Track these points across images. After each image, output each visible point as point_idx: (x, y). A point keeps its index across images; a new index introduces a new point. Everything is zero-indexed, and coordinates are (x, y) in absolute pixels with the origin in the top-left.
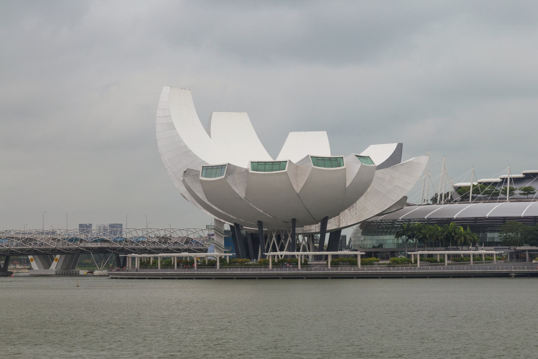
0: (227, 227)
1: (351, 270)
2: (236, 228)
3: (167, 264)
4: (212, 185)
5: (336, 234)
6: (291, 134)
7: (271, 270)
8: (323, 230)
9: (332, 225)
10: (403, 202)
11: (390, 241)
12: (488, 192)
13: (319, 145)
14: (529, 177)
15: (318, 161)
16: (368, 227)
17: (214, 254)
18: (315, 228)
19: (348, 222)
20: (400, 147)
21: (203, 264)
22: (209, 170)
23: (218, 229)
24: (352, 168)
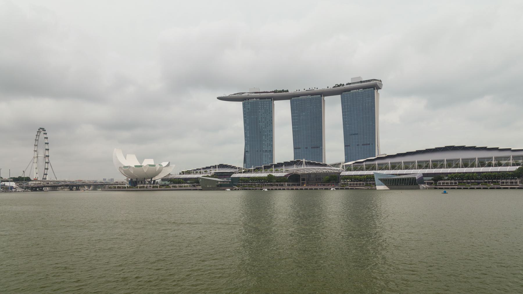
0: (129, 179)
1: (157, 189)
2: (131, 180)
3: (115, 188)
4: (125, 170)
5: (154, 181)
6: (145, 160)
7: (139, 189)
8: (151, 180)
9: (153, 179)
10: (169, 174)
11: (167, 183)
12: (189, 172)
13: (151, 162)
14: (197, 169)
15: (150, 165)
16: (163, 180)
17: (126, 185)
18: (150, 180)
19: (158, 179)
20: (169, 163)
21: (123, 188)
22: (125, 167)
23: (127, 180)
24: (158, 167)
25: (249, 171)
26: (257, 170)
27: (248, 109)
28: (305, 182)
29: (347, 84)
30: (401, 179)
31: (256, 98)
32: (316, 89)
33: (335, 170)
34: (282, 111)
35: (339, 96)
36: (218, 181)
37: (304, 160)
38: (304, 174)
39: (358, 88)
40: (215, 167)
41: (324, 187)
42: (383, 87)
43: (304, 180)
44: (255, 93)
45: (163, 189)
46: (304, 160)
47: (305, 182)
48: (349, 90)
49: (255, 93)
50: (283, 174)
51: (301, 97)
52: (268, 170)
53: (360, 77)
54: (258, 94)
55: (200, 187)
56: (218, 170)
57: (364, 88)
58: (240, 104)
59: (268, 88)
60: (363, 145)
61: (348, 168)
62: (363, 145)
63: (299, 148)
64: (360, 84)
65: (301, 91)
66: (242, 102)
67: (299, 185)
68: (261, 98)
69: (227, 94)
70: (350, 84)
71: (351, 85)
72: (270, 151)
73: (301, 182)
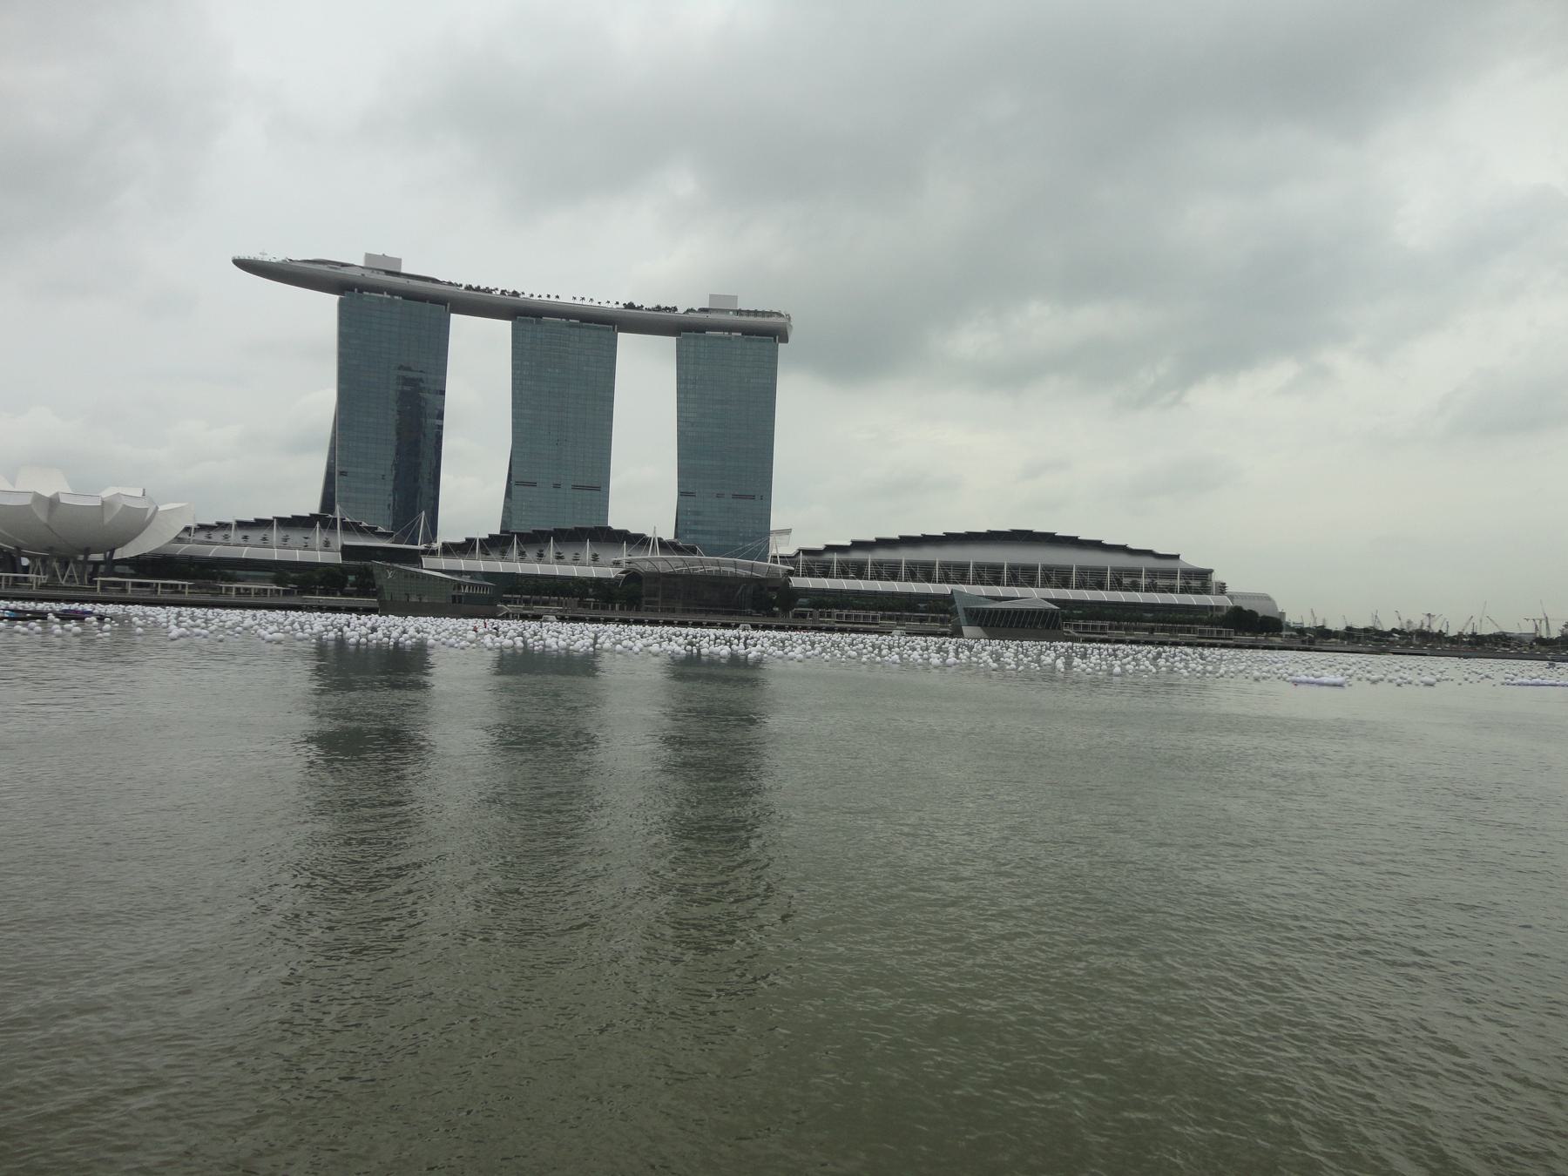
28: (659, 599)
29: (692, 310)
30: (1003, 611)
31: (392, 291)
32: (595, 303)
33: (744, 567)
35: (670, 342)
38: (657, 577)
39: (730, 328)
42: (790, 339)
44: (388, 273)
45: (195, 598)
47: (659, 599)
49: (388, 273)
50: (612, 573)
52: (531, 554)
53: (736, 298)
55: (372, 602)
57: (748, 331)
58: (332, 300)
63: (534, 484)
66: (336, 298)
67: (638, 610)
69: (274, 254)
71: (711, 316)
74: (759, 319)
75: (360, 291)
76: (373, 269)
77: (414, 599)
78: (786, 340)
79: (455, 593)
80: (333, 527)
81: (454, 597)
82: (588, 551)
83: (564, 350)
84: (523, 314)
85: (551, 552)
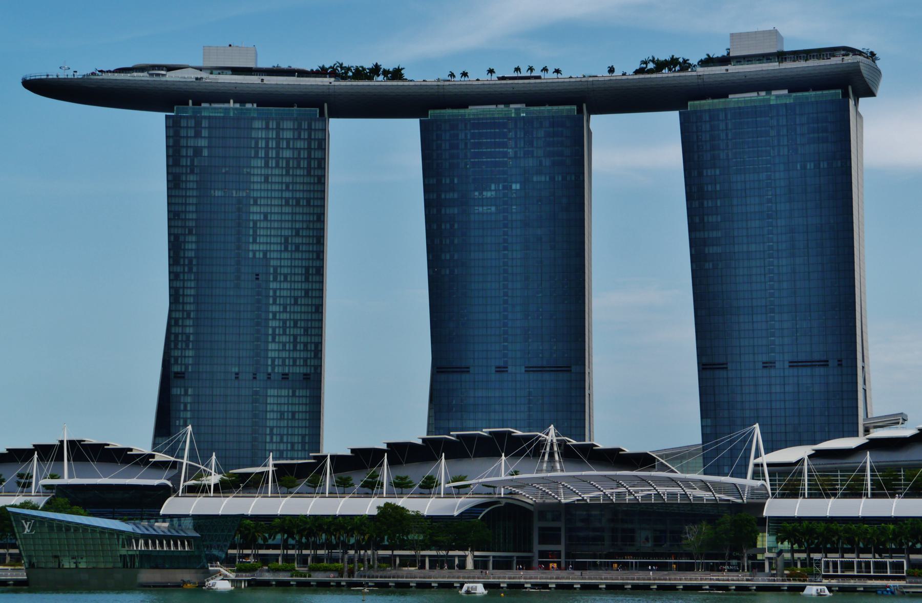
25: (250, 484)
26: (288, 478)
27: (197, 151)
29: (708, 61)
31: (242, 97)
32: (550, 76)
34: (375, 177)
36: (129, 538)
37: (551, 435)
40: (47, 453)
41: (575, 578)
43: (549, 536)
44: (236, 71)
46: (551, 435)
47: (562, 548)
48: (721, 90)
49: (236, 71)
50: (454, 506)
51: (473, 110)
52: (358, 478)
54: (254, 79)
56: (69, 476)
58: (154, 123)
59: (306, 50)
60: (794, 364)
61: (787, 481)
62: (794, 364)
64: (774, 66)
65: (472, 77)
67: (527, 564)
68: (266, 99)
70: (725, 60)
71: (732, 68)
72: (306, 376)
73: (537, 547)
74: (813, 63)
75: (197, 103)
76: (212, 70)
77: (68, 564)
78: (871, 93)
79: (123, 552)
80: (60, 458)
81: (123, 557)
82: (442, 468)
83: (503, 156)
84: (433, 107)
85: (385, 474)
